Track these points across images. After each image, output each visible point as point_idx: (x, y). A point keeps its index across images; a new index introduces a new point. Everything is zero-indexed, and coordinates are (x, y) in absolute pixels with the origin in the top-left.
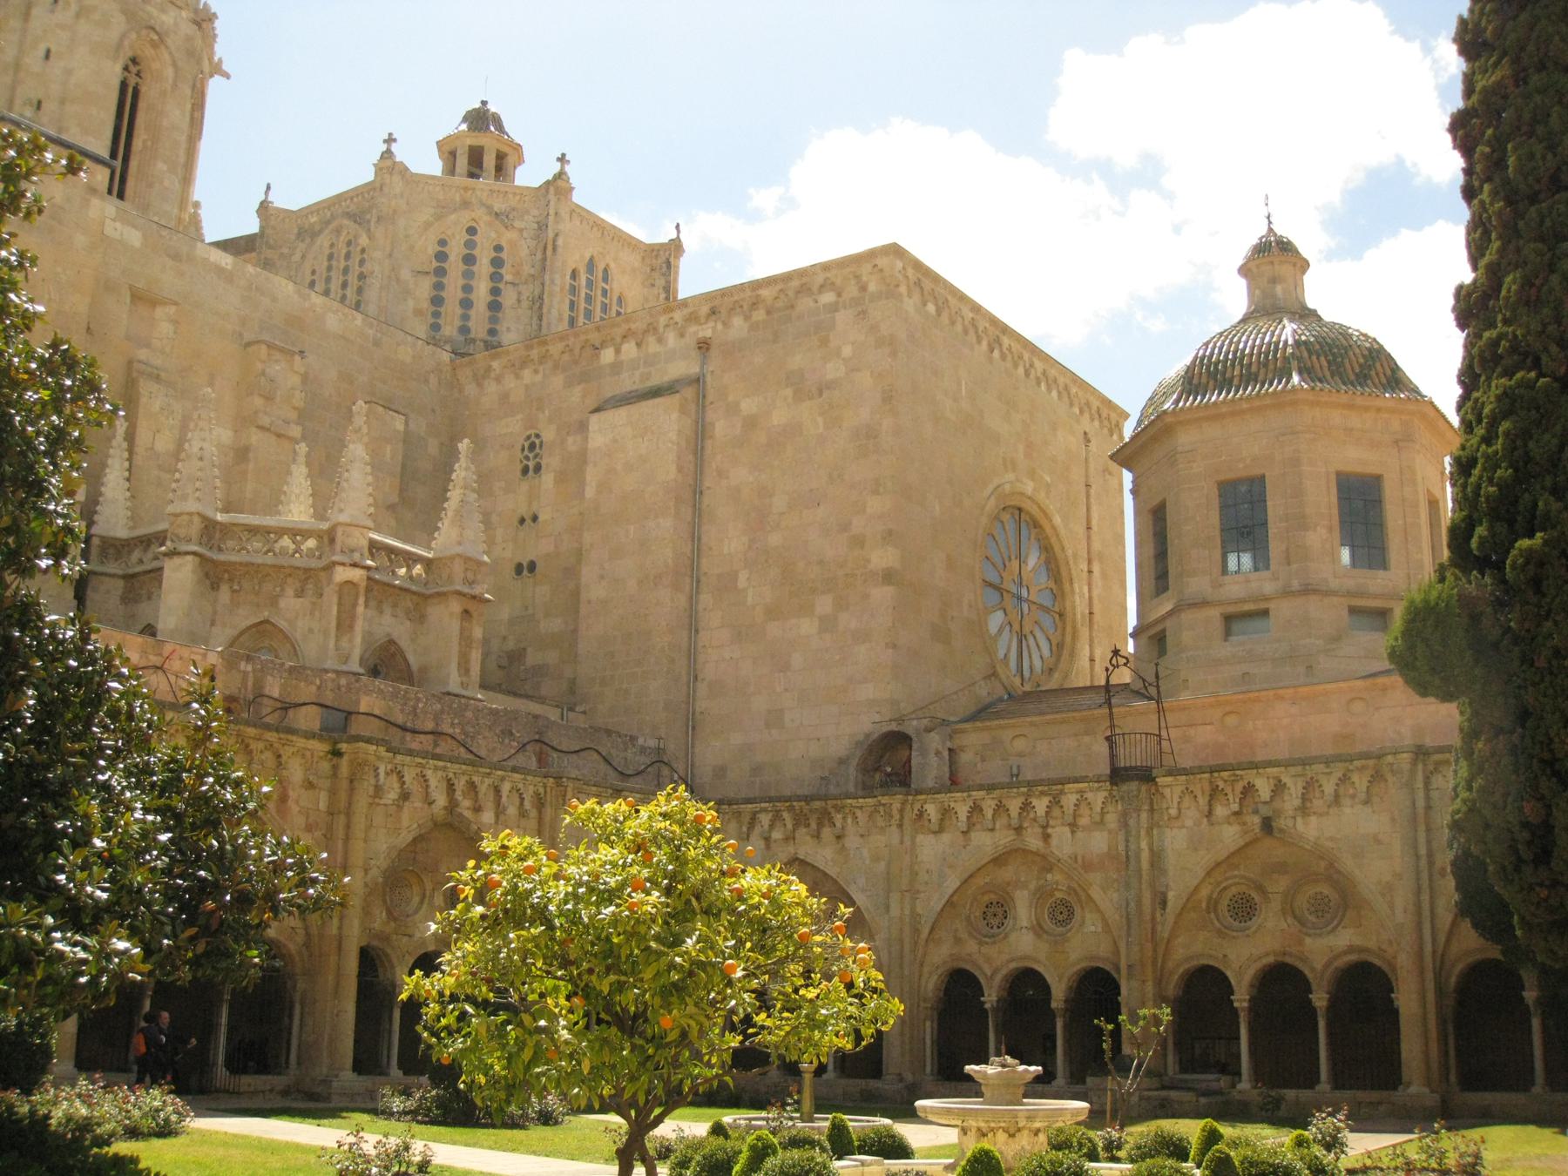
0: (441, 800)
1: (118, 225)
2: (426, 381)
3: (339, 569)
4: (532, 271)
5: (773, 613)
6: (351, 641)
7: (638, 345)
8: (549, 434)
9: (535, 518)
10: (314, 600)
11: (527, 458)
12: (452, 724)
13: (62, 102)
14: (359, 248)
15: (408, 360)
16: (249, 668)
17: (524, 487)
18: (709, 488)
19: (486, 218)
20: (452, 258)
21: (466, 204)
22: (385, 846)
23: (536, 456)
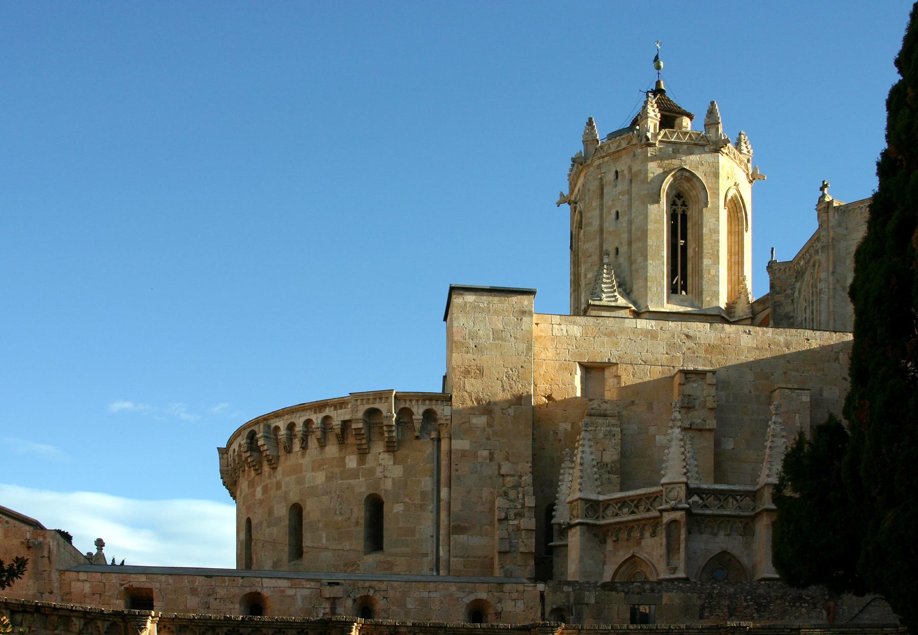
2: (837, 359)
3: (665, 514)
6: (679, 559)
12: (746, 600)
13: (630, 243)
16: (570, 589)
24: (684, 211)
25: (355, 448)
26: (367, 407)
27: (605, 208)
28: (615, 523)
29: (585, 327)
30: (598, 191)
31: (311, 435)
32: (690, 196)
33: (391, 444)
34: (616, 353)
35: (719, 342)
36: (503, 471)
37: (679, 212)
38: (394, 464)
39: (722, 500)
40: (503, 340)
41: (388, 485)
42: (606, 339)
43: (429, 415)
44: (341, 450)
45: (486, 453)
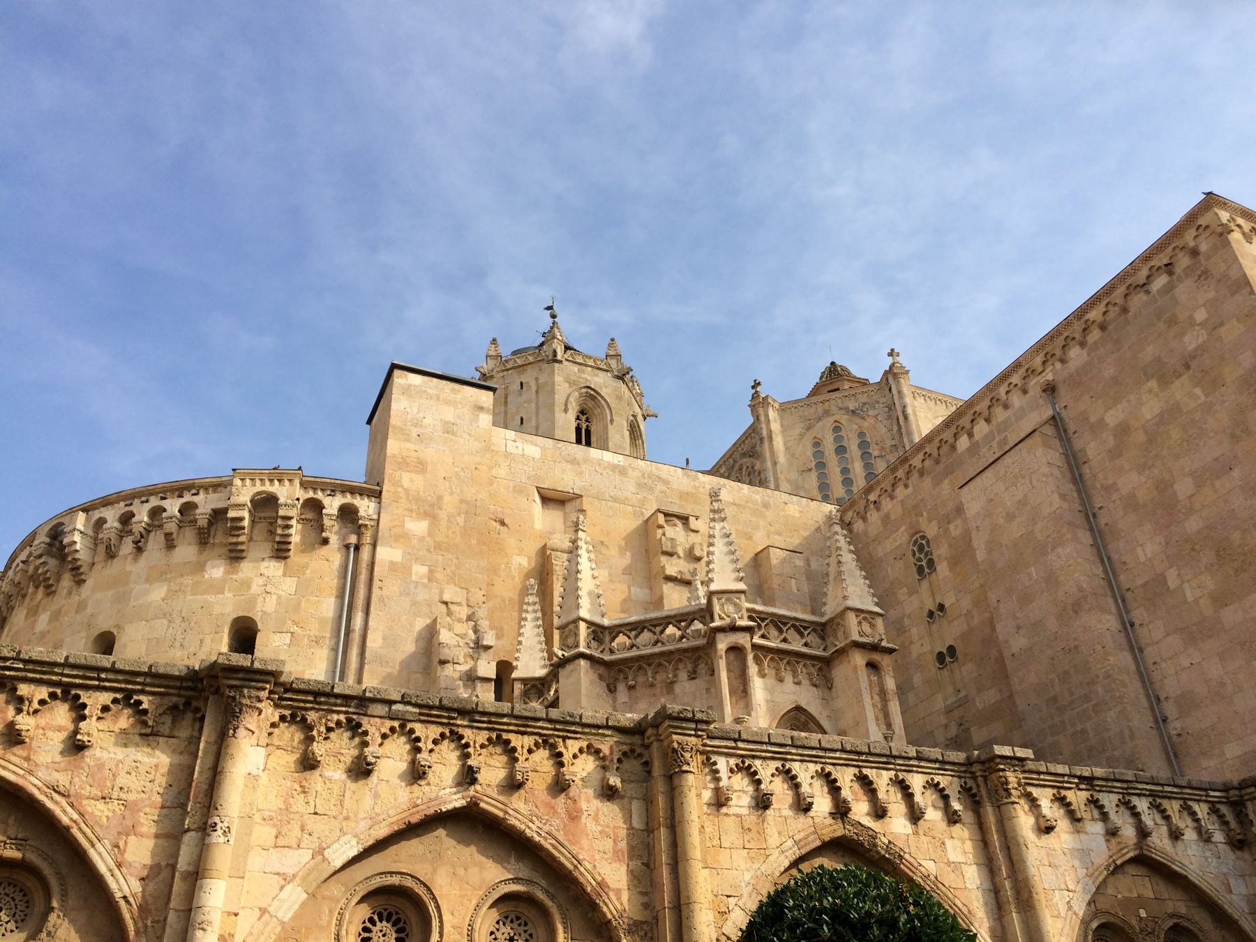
0: (822, 805)
1: (519, 444)
3: (720, 636)
4: (893, 443)
5: (1221, 599)
7: (988, 420)
8: (931, 530)
9: (941, 607)
10: (708, 678)
11: (920, 560)
14: (757, 473)
15: (797, 515)
17: (925, 584)
18: (1100, 508)
19: (846, 417)
20: (827, 453)
21: (827, 413)
22: (747, 876)
23: (926, 555)
24: (587, 426)
25: (225, 550)
26: (259, 487)
27: (509, 415)
28: (632, 659)
29: (543, 449)
30: (503, 400)
31: (156, 531)
32: (594, 414)
33: (284, 547)
34: (578, 483)
35: (694, 491)
36: (446, 598)
37: (584, 426)
38: (284, 575)
39: (785, 629)
40: (454, 433)
41: (270, 605)
42: (569, 466)
43: (348, 514)
44: (201, 552)
45: (423, 570)
